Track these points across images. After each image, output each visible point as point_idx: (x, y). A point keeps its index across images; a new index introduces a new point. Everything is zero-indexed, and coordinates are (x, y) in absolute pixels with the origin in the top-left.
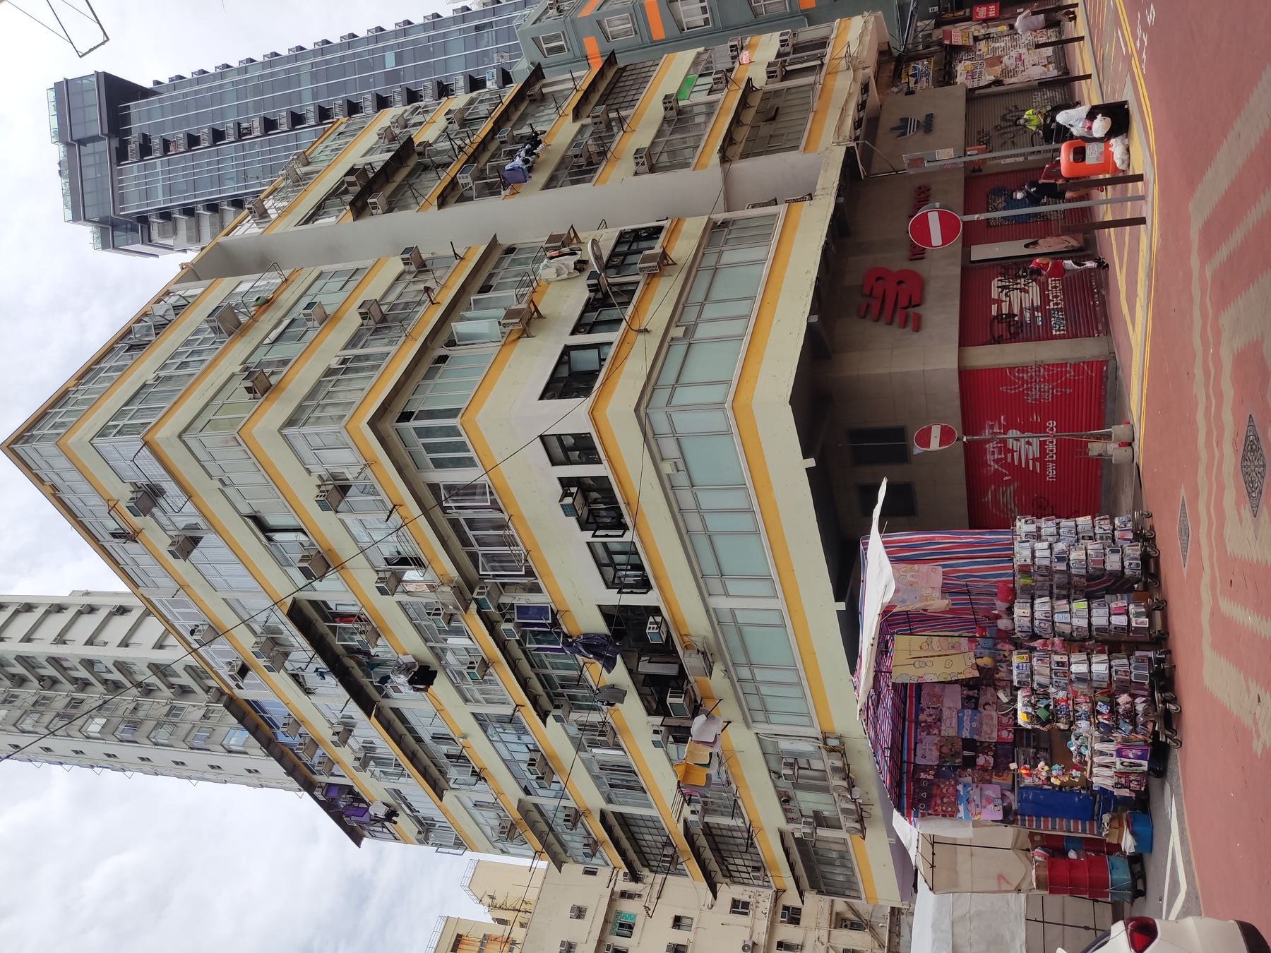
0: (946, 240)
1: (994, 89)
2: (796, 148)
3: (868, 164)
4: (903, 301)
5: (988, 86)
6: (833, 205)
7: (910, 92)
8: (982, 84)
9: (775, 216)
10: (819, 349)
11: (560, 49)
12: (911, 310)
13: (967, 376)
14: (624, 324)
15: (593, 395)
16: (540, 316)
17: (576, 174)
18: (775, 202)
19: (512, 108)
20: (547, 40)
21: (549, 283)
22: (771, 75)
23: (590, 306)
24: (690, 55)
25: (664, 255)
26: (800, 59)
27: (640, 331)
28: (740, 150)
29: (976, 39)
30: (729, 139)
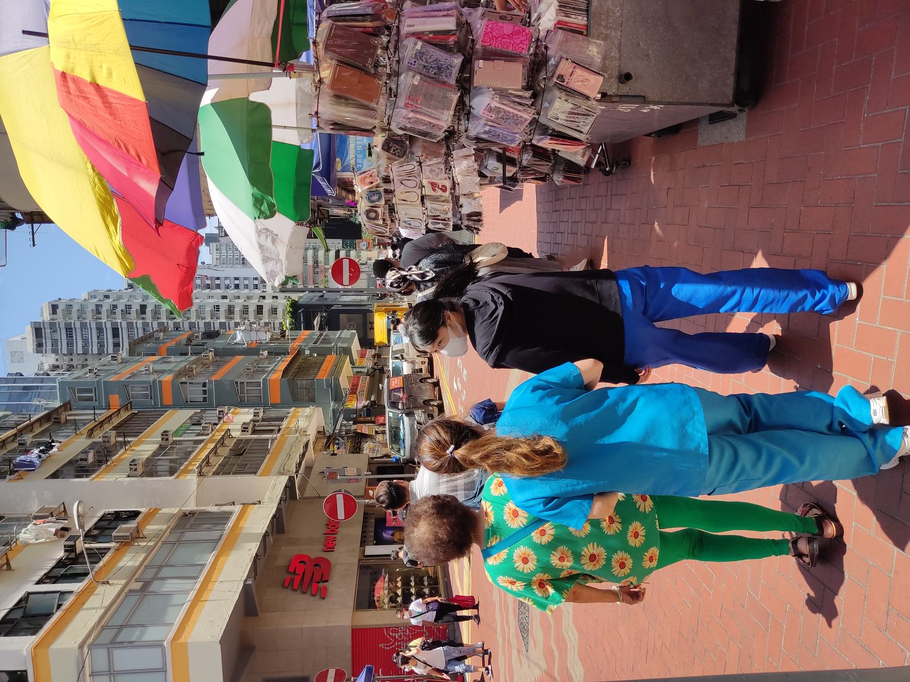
0: (348, 514)
1: (385, 459)
2: (255, 473)
3: (303, 488)
4: (317, 577)
5: (382, 457)
6: (275, 509)
7: (334, 454)
8: (379, 455)
9: (231, 513)
10: (249, 605)
11: (90, 399)
12: (321, 585)
13: (358, 634)
14: (90, 575)
15: (42, 633)
16: (9, 568)
17: (78, 471)
18: (233, 503)
19: (37, 425)
20: (80, 391)
21: (26, 545)
22: (245, 429)
23: (60, 564)
24: (189, 413)
25: (138, 530)
26: (265, 426)
27: (104, 583)
28: (214, 470)
29: (377, 432)
30: (207, 461)
